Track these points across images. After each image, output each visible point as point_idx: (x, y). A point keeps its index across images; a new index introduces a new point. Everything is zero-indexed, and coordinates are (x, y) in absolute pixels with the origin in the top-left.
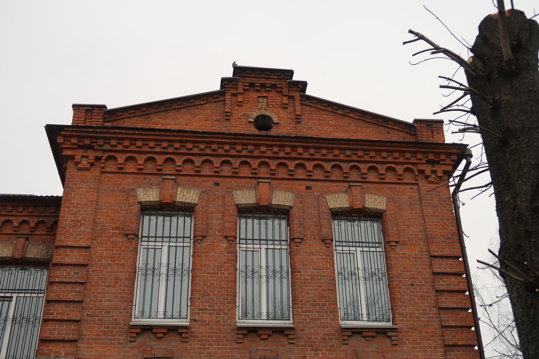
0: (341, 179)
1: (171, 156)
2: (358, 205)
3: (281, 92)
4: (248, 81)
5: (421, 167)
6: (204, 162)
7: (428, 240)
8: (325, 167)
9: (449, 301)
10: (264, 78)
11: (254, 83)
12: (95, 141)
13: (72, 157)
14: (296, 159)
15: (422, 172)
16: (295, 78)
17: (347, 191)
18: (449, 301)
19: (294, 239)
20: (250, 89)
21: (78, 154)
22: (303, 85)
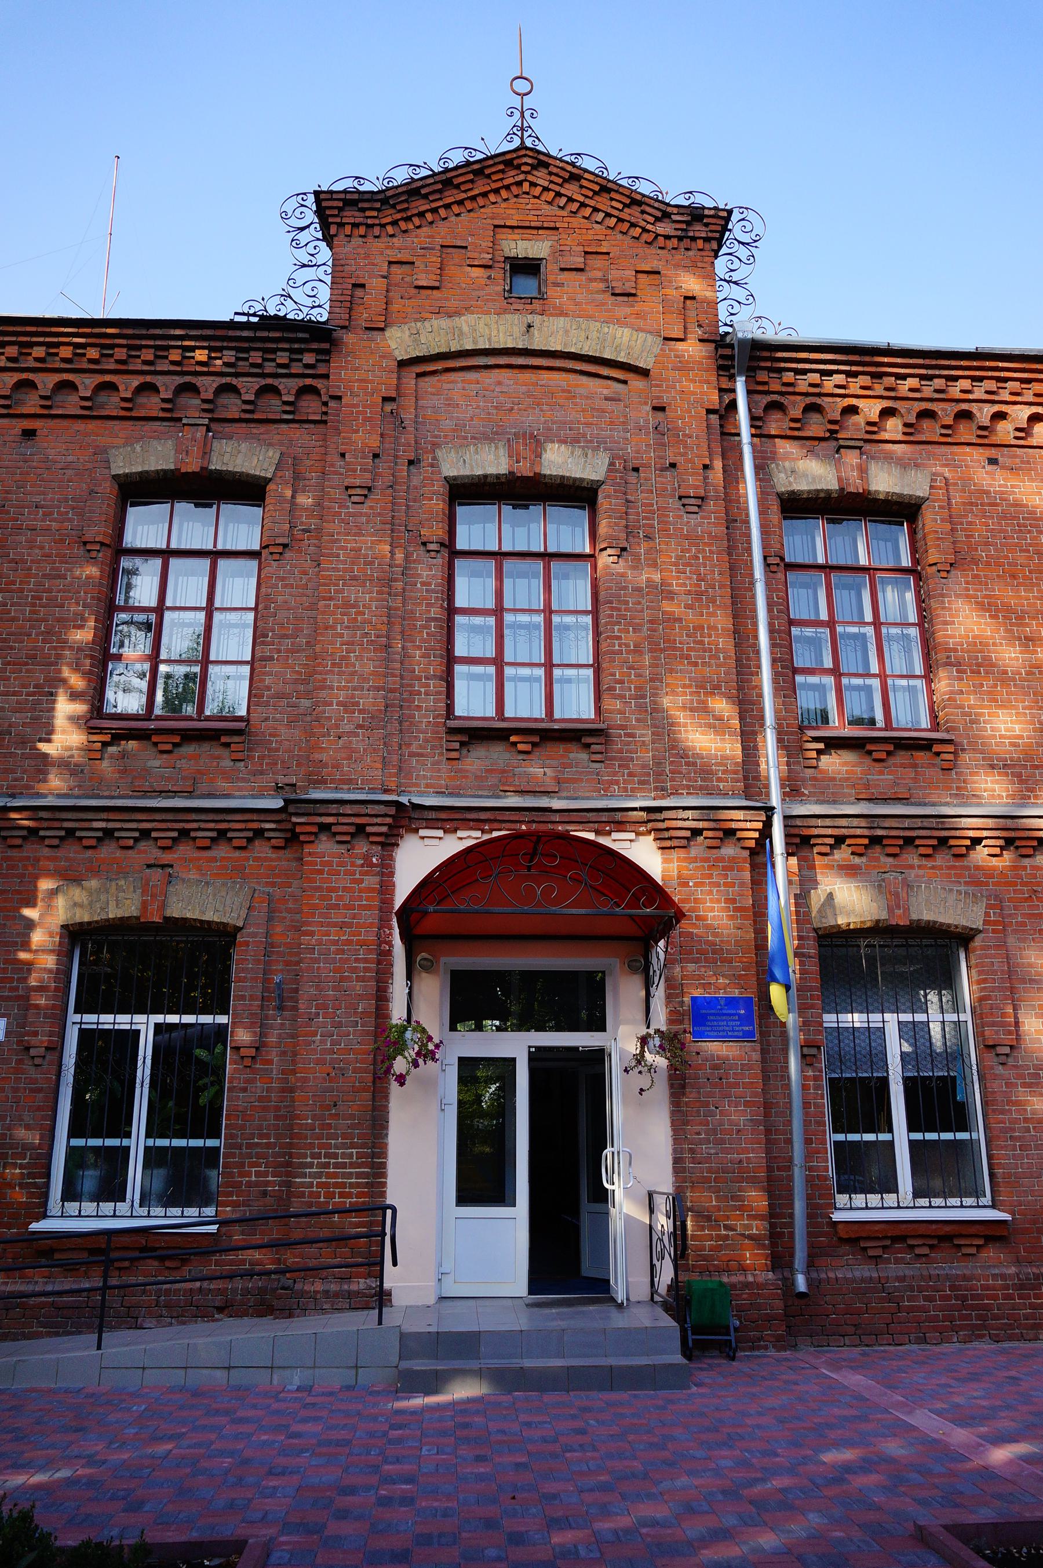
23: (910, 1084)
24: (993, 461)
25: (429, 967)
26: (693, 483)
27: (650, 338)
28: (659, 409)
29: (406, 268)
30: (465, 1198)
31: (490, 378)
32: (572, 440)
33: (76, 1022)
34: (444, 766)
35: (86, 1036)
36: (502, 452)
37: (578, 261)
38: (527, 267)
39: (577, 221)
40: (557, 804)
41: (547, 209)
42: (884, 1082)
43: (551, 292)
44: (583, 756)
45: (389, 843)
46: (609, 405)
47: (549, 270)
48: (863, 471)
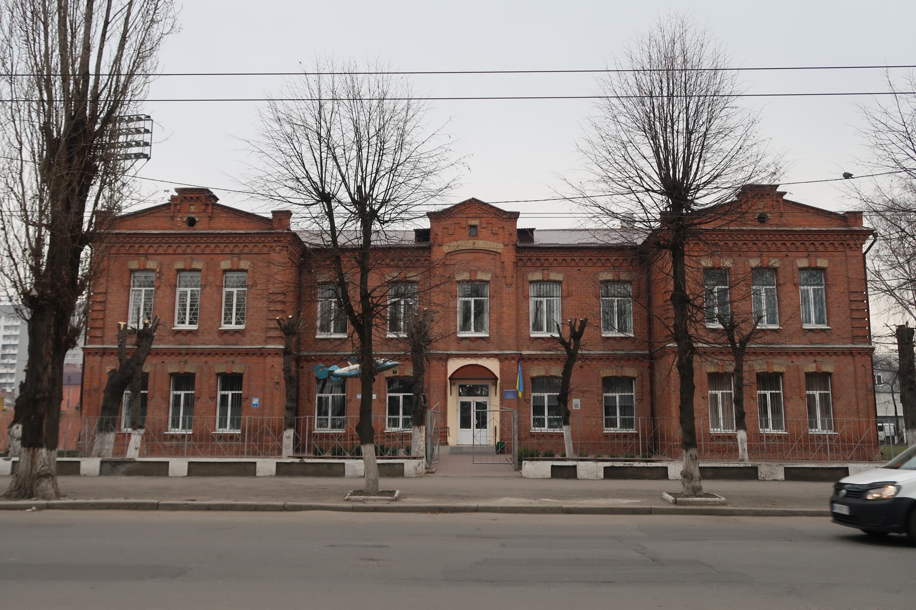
0: (804, 250)
2: (813, 265)
5: (848, 242)
7: (849, 283)
9: (856, 315)
14: (781, 240)
15: (848, 245)
16: (779, 190)
17: (807, 257)
18: (856, 315)
23: (549, 406)
24: (579, 270)
25: (454, 384)
26: (509, 281)
27: (501, 245)
28: (503, 263)
29: (446, 229)
30: (462, 427)
31: (466, 255)
32: (484, 271)
33: (388, 395)
34: (457, 345)
35: (390, 397)
36: (468, 274)
37: (485, 226)
38: (474, 227)
39: (485, 215)
40: (479, 353)
41: (478, 212)
42: (544, 407)
43: (479, 234)
44: (484, 342)
45: (446, 361)
46: (492, 261)
47: (479, 228)
48: (548, 274)
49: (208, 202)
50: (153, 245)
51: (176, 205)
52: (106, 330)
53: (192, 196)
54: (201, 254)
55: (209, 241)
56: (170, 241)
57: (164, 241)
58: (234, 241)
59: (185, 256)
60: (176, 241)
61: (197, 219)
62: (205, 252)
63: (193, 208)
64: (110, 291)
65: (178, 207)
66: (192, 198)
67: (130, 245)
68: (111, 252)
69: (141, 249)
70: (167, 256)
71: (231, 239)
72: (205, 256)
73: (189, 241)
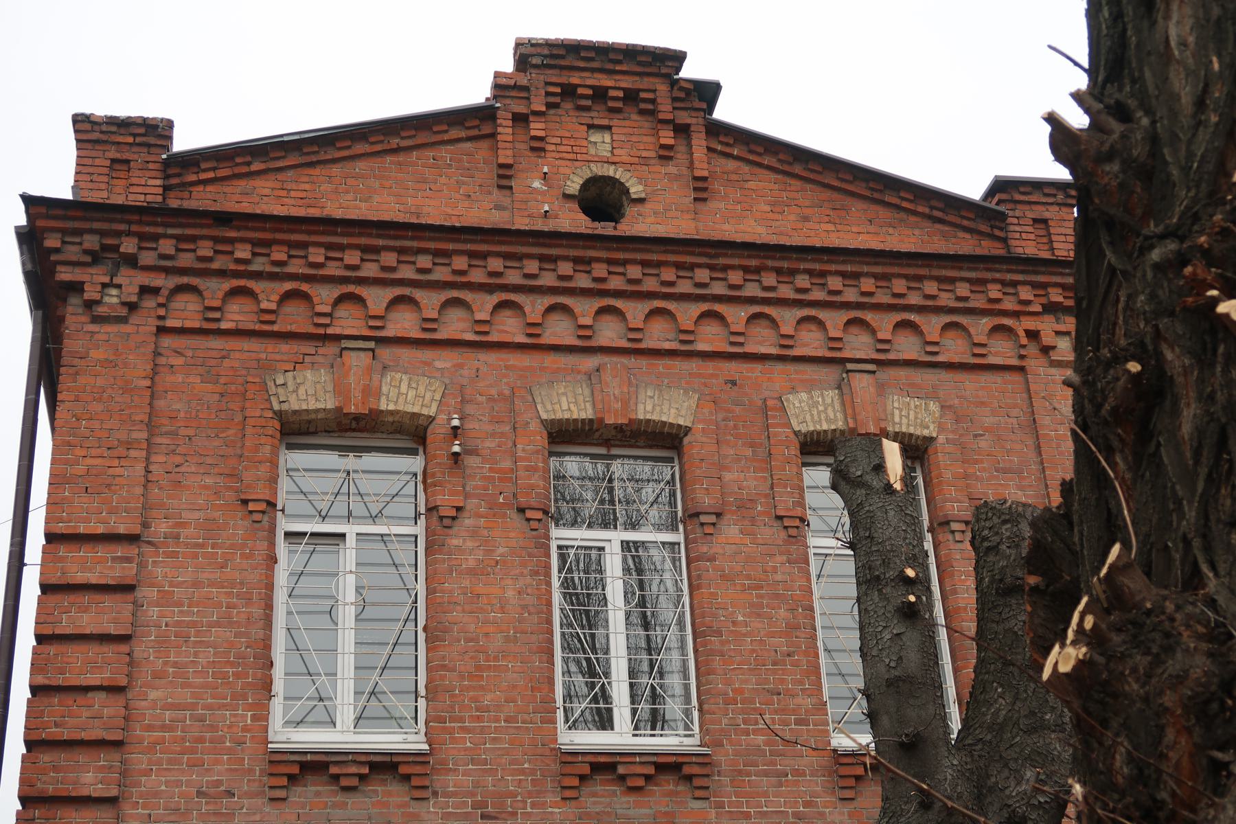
1: (407, 291)
3: (652, 113)
4: (624, 85)
6: (602, 311)
8: (924, 328)
10: (601, 71)
11: (607, 88)
12: (227, 248)
13: (77, 287)
19: (697, 515)
20: (593, 108)
21: (93, 277)
22: (708, 92)
49: (683, 118)
50: (418, 294)
51: (520, 119)
52: (139, 760)
53: (606, 81)
54: (672, 353)
55: (718, 289)
56: (513, 278)
57: (478, 276)
58: (851, 295)
59: (592, 362)
60: (548, 280)
61: (636, 190)
62: (701, 346)
63: (601, 143)
64: (161, 528)
65: (537, 128)
66: (600, 94)
67: (288, 286)
68: (170, 323)
69: (343, 312)
70: (491, 357)
71: (835, 283)
72: (693, 365)
73: (615, 283)
